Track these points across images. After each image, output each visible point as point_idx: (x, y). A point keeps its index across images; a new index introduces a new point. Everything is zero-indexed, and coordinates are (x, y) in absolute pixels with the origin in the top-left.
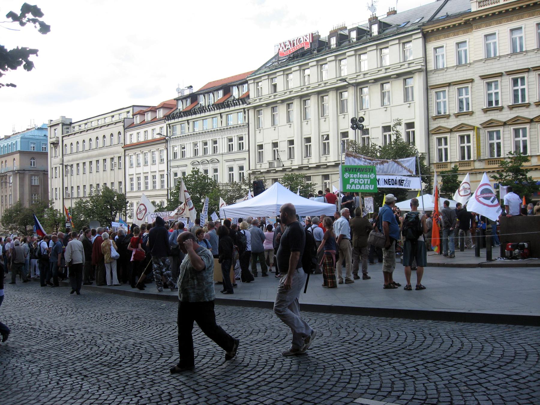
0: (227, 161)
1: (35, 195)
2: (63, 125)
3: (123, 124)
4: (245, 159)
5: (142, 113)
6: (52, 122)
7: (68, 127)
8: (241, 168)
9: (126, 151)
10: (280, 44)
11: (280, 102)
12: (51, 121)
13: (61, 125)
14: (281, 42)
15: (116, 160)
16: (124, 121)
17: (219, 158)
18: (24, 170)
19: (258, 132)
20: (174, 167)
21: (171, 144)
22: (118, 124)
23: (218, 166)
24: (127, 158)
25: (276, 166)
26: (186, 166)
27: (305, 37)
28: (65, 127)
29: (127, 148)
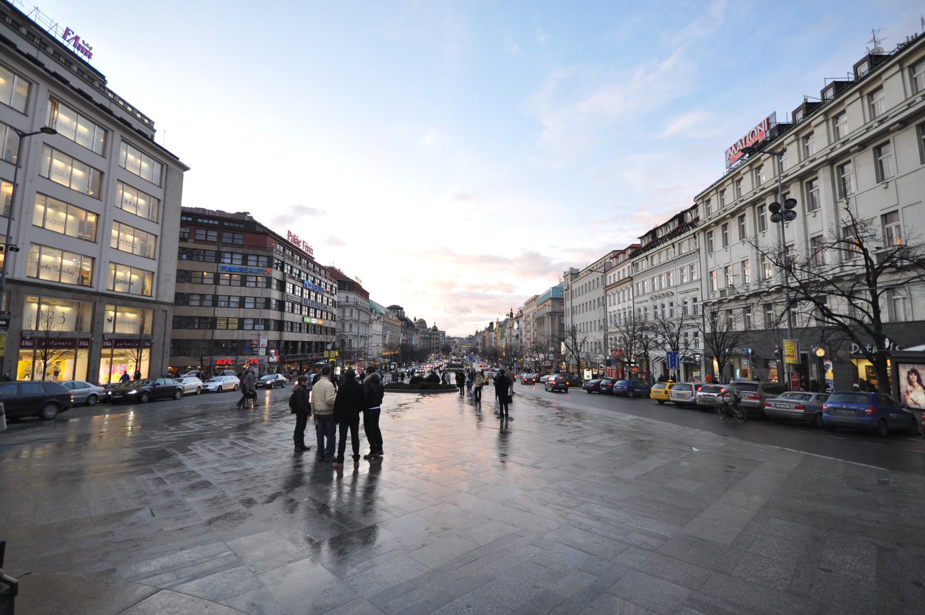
0: (681, 293)
4: (698, 289)
5: (617, 257)
8: (695, 300)
10: (731, 148)
11: (729, 216)
14: (731, 145)
15: (601, 300)
17: (674, 291)
19: (709, 257)
20: (638, 303)
21: (635, 282)
23: (673, 299)
24: (608, 298)
25: (727, 294)
26: (647, 301)
27: (759, 128)
28: (573, 276)
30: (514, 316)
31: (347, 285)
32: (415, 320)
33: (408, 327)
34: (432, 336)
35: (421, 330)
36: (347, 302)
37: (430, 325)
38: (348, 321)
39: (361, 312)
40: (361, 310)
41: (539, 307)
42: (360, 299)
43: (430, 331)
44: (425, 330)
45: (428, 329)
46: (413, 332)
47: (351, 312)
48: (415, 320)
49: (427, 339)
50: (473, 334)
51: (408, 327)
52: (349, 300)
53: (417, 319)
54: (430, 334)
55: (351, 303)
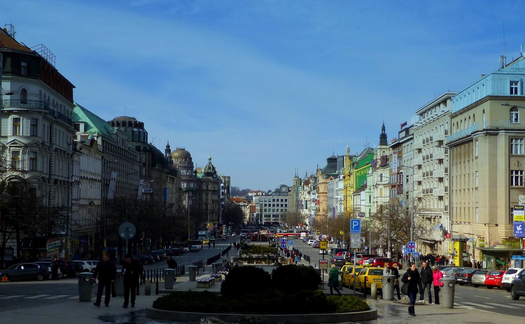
1: (517, 172)
18: (498, 129)
30: (390, 141)
31: (23, 64)
32: (168, 150)
33: (153, 165)
34: (204, 187)
39: (55, 126)
41: (455, 120)
42: (52, 97)
46: (164, 176)
48: (168, 150)
50: (290, 183)
52: (29, 98)
53: (172, 149)
55: (33, 105)
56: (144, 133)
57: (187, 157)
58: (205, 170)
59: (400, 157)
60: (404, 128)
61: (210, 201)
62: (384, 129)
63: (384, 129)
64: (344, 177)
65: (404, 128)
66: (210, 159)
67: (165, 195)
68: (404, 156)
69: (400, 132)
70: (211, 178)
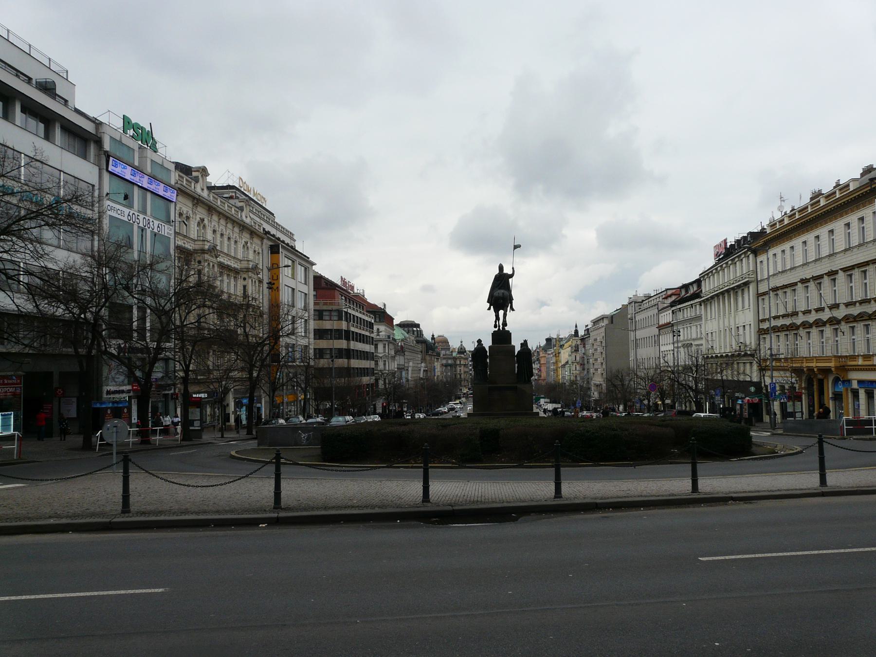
2: (635, 302)
3: (657, 306)
6: (631, 299)
7: (641, 304)
9: (661, 331)
12: (630, 298)
13: (633, 303)
16: (658, 304)
22: (654, 308)
24: (660, 337)
28: (637, 304)
29: (661, 327)
32: (433, 338)
33: (427, 352)
34: (458, 362)
35: (443, 352)
36: (378, 335)
37: (454, 344)
38: (381, 358)
39: (390, 344)
40: (391, 343)
43: (454, 354)
44: (448, 352)
45: (452, 352)
47: (384, 347)
48: (433, 338)
49: (451, 365)
51: (427, 352)
54: (455, 359)
55: (384, 337)
56: (420, 331)
57: (445, 342)
58: (458, 350)
59: (584, 347)
60: (587, 328)
61: (462, 372)
62: (576, 326)
63: (576, 326)
64: (556, 354)
65: (587, 328)
66: (461, 342)
67: (434, 371)
68: (586, 346)
69: (585, 330)
70: (463, 356)
